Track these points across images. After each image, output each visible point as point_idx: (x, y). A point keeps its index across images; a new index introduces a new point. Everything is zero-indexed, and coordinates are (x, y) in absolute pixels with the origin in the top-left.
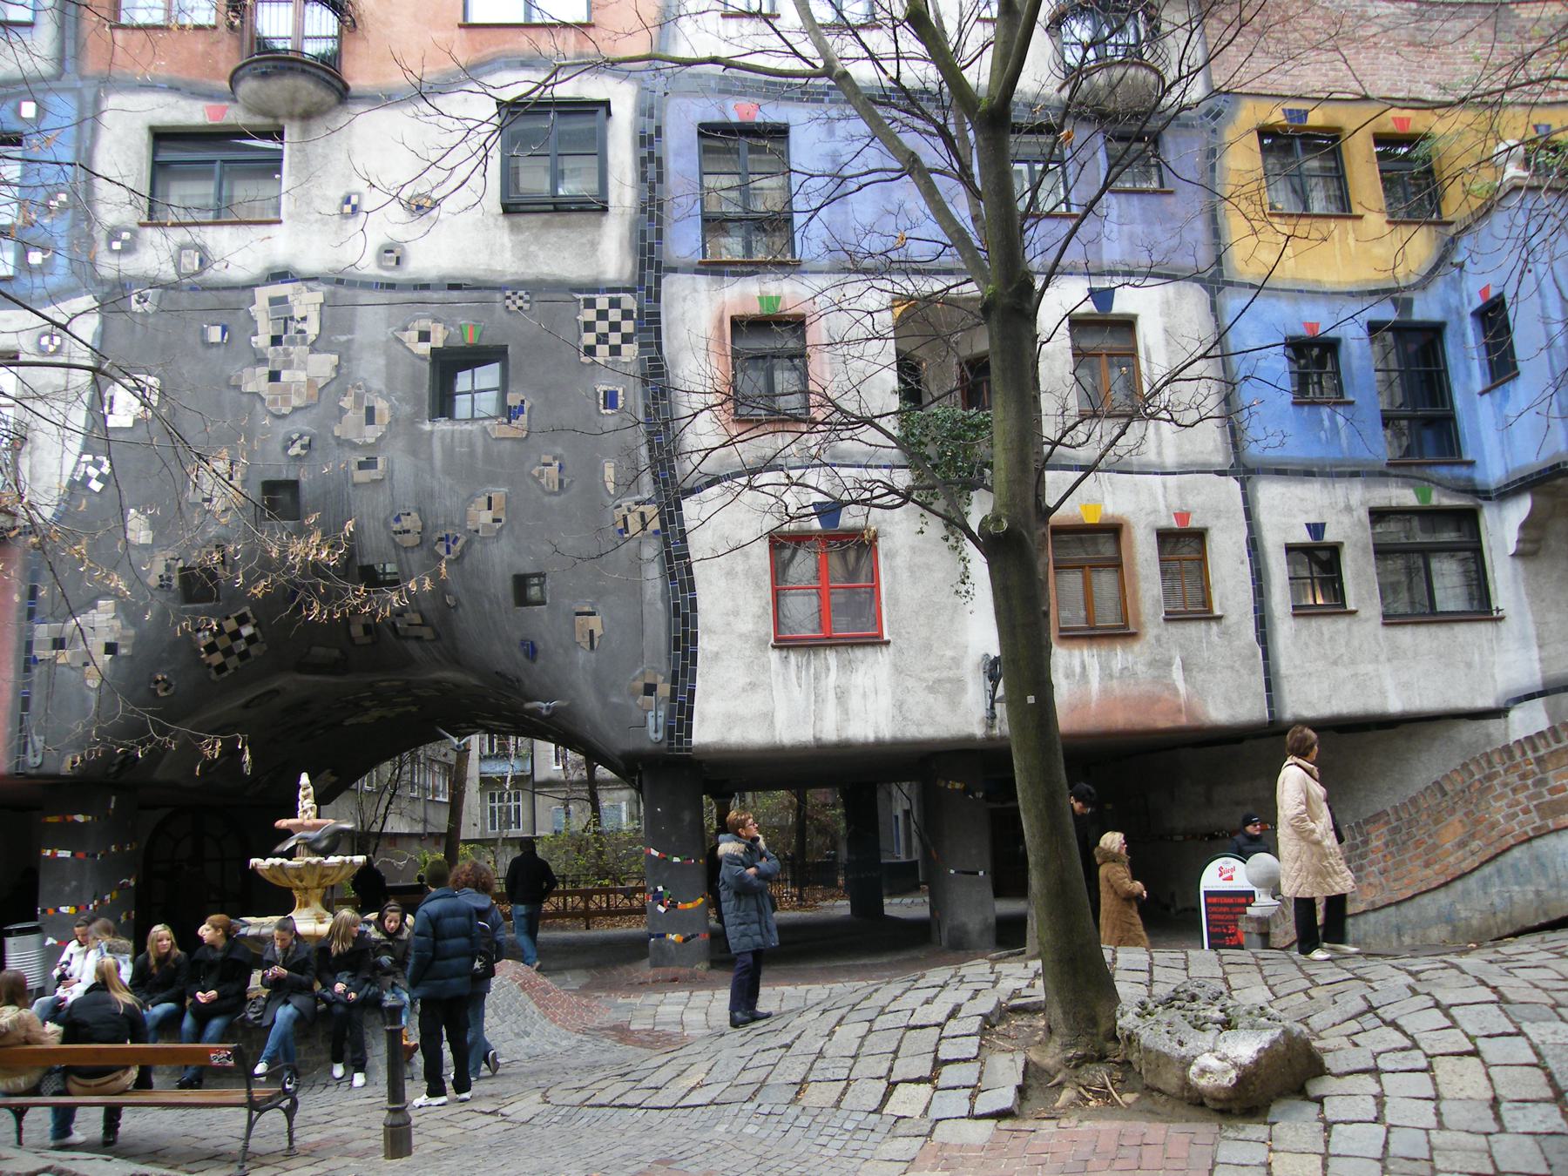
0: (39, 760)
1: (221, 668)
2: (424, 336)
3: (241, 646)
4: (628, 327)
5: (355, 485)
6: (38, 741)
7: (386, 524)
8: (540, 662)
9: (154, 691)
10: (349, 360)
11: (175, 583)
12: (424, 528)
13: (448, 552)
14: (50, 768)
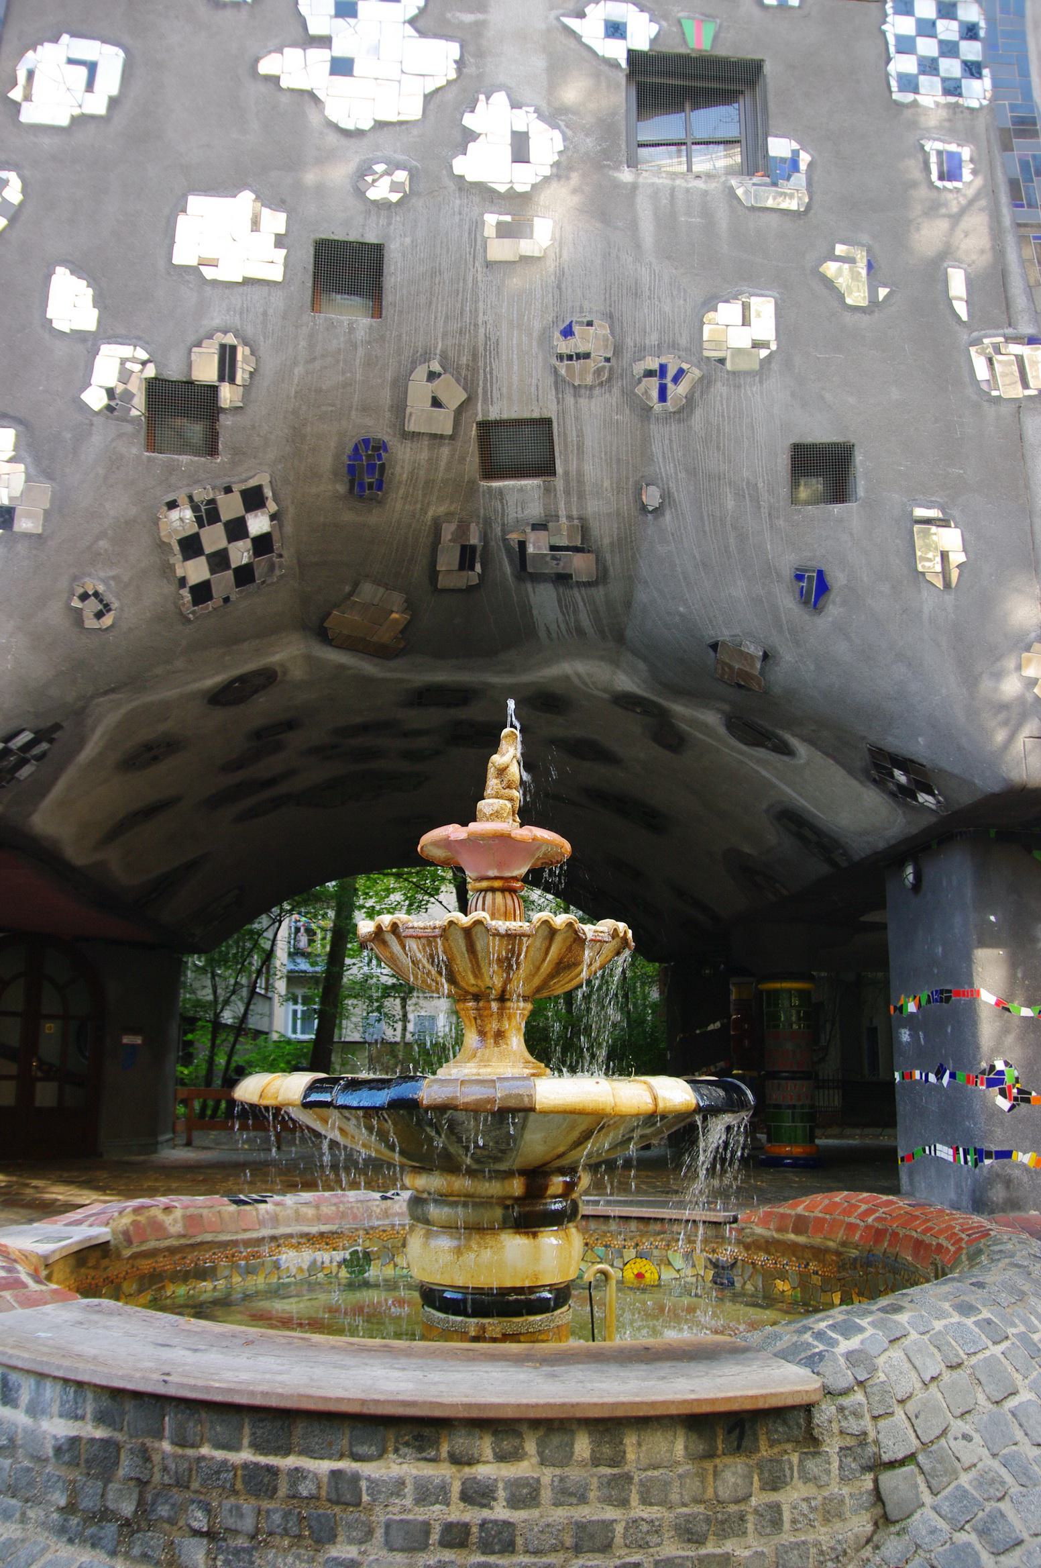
1: (202, 592)
2: (615, 30)
3: (241, 553)
4: (972, 50)
5: (489, 265)
7: (544, 338)
8: (834, 609)
9: (78, 615)
10: (480, 54)
13: (663, 396)
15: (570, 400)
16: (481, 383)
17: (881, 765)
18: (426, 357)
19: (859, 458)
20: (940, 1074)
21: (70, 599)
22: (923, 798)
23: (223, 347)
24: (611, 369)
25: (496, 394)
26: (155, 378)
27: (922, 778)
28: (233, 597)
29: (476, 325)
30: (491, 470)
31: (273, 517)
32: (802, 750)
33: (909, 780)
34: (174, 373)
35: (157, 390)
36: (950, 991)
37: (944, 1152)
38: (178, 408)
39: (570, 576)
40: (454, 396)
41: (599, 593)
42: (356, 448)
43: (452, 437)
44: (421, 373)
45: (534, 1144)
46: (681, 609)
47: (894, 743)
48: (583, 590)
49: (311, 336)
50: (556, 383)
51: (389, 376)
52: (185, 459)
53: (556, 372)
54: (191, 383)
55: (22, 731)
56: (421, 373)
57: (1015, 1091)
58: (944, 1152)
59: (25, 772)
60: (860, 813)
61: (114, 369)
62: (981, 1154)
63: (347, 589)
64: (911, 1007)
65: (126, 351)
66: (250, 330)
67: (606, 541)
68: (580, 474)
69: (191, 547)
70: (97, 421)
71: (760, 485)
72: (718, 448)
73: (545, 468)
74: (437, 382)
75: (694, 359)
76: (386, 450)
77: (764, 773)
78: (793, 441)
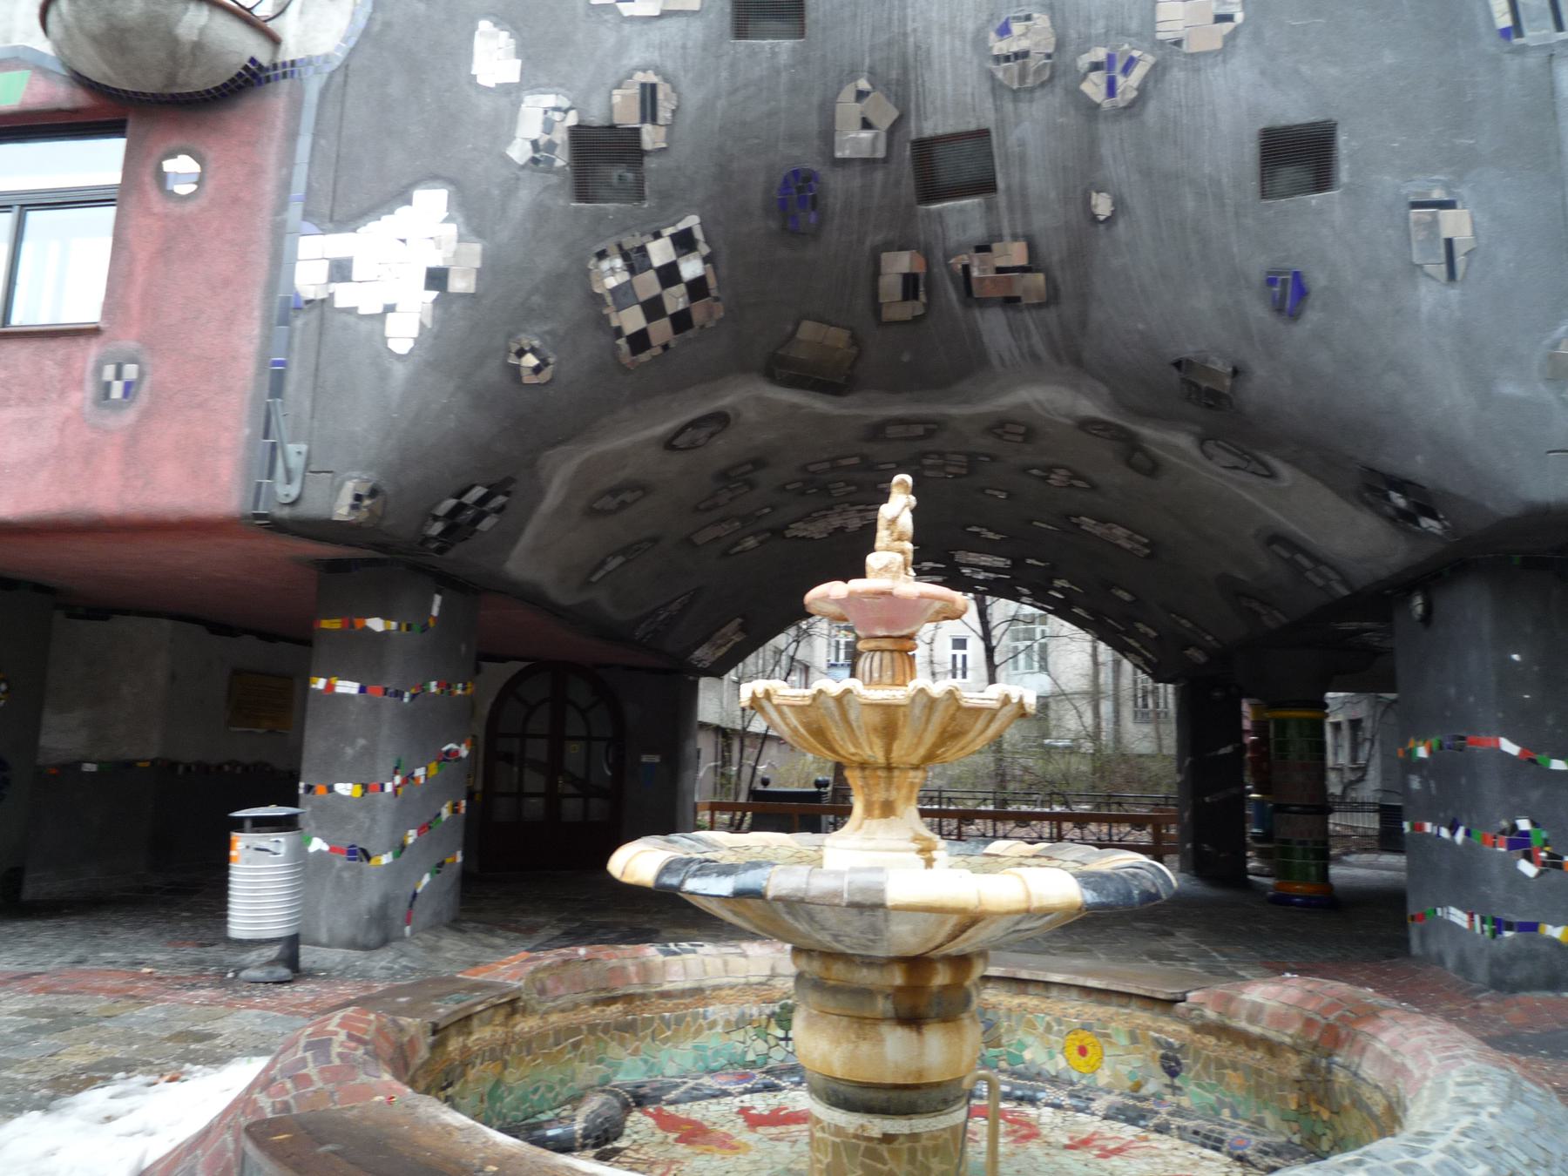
0: (294, 490)
1: (639, 341)
3: (676, 299)
6: (295, 452)
7: (979, 42)
8: (1313, 316)
11: (561, 160)
12: (1060, 45)
13: (1111, 89)
14: (313, 508)
15: (1009, 106)
16: (913, 97)
17: (1374, 486)
18: (853, 75)
19: (1342, 138)
20: (1453, 829)
21: (507, 356)
22: (1426, 522)
23: (643, 85)
24: (1053, 66)
25: (929, 108)
26: (578, 126)
27: (1424, 502)
28: (672, 345)
29: (905, 35)
30: (931, 191)
31: (706, 260)
32: (1286, 472)
33: (1409, 503)
34: (596, 117)
35: (579, 135)
36: (1463, 738)
37: (1458, 917)
38: (601, 154)
39: (1018, 299)
40: (885, 115)
41: (1050, 315)
42: (786, 181)
43: (885, 160)
44: (848, 94)
45: (905, 937)
46: (1141, 326)
47: (1389, 461)
48: (1034, 313)
49: (732, 65)
50: (993, 90)
51: (816, 99)
52: (611, 206)
53: (992, 76)
54: (612, 127)
55: (472, 487)
56: (848, 94)
57: (1543, 854)
58: (1458, 917)
59: (486, 524)
60: (1356, 540)
61: (539, 121)
62: (1499, 925)
63: (789, 328)
64: (1422, 752)
65: (550, 100)
66: (670, 66)
67: (1055, 258)
68: (1023, 187)
69: (622, 295)
70: (523, 174)
71: (1225, 180)
72: (1175, 142)
73: (985, 186)
74: (866, 101)
75: (1146, 45)
76: (816, 180)
77: (1248, 497)
78: (1262, 126)
